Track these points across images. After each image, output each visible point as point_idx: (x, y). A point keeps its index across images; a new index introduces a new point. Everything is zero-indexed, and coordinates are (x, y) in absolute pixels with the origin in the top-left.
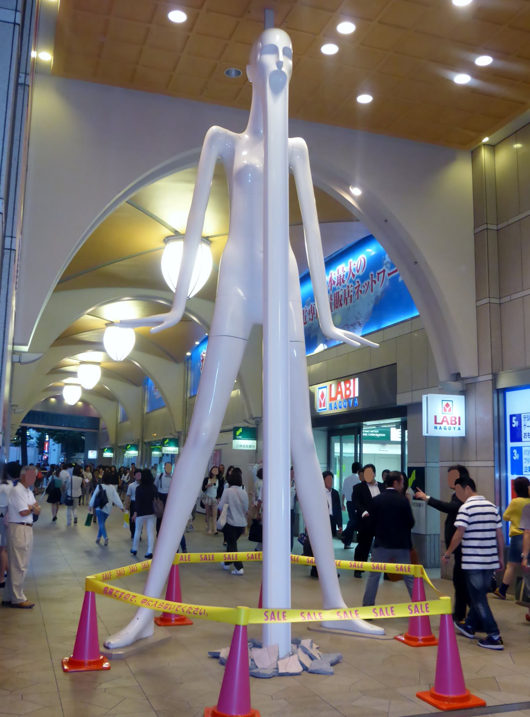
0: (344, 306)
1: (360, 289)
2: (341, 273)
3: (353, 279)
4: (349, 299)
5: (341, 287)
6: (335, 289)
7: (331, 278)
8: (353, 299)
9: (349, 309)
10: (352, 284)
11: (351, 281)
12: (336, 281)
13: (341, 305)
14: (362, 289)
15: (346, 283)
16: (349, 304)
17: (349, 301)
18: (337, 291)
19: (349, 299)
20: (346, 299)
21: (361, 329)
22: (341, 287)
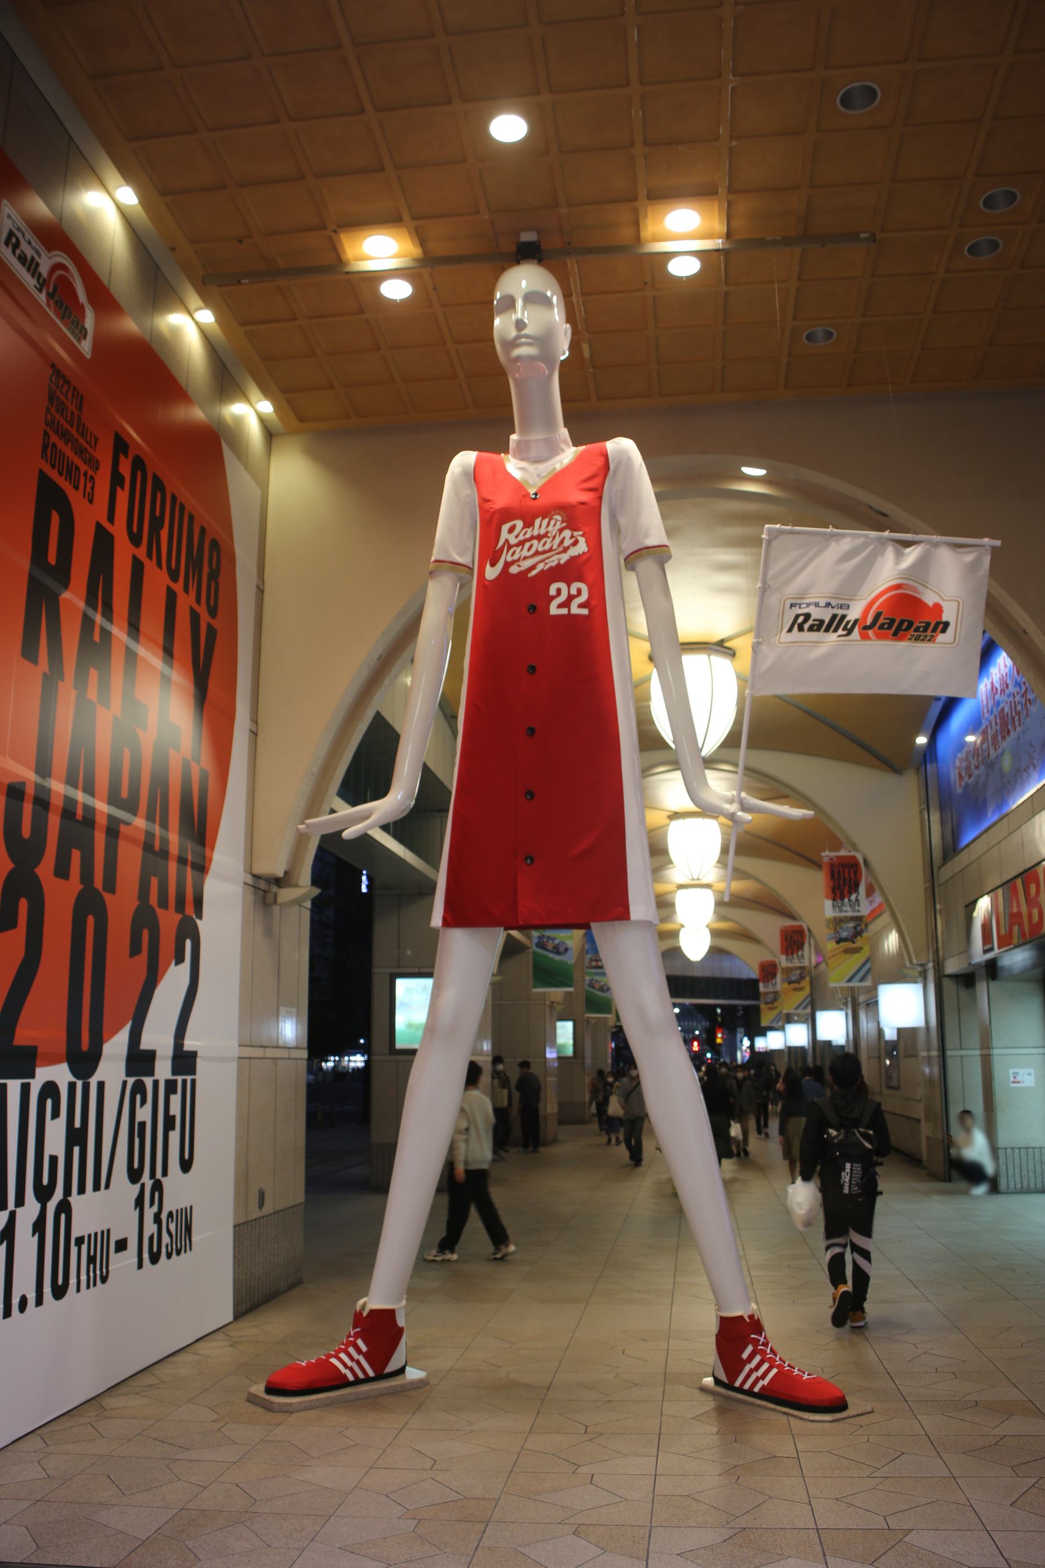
0: (1013, 734)
1: (1029, 696)
2: (1004, 671)
3: (1019, 679)
4: (1017, 718)
5: (1005, 698)
6: (998, 703)
7: (992, 683)
8: (1023, 714)
9: (1018, 739)
10: (1018, 689)
11: (1017, 684)
12: (997, 685)
13: (1009, 732)
14: (1030, 696)
15: (1012, 689)
16: (1018, 729)
17: (1017, 724)
18: (1001, 706)
19: (1017, 718)
20: (1013, 718)
21: (1035, 775)
22: (1005, 698)
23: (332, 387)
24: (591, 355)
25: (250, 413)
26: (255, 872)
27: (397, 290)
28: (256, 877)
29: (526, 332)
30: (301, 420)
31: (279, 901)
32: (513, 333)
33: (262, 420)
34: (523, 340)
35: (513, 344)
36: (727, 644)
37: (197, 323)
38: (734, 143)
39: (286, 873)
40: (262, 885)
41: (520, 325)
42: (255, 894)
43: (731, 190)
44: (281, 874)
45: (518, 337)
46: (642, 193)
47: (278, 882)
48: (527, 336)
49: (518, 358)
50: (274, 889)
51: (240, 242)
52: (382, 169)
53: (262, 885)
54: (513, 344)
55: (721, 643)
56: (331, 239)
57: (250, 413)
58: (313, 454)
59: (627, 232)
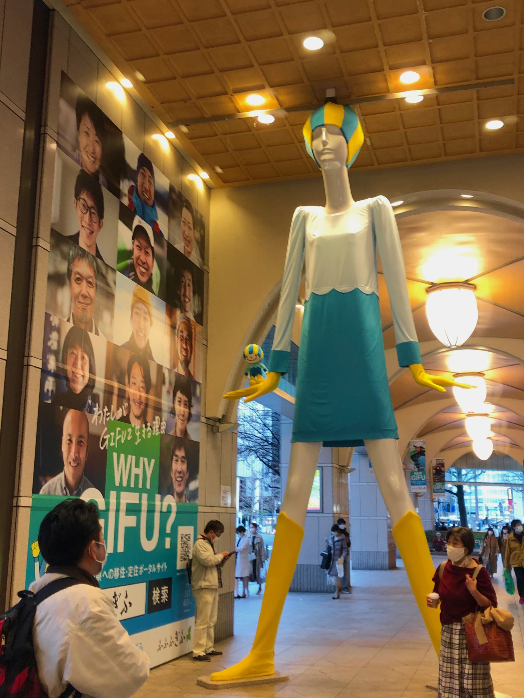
23: (239, 166)
24: (372, 144)
25: (197, 180)
26: (207, 416)
27: (266, 118)
28: (208, 418)
29: (327, 147)
30: (225, 182)
31: (219, 431)
32: (321, 148)
33: (205, 182)
34: (326, 151)
35: (321, 153)
36: (470, 282)
37: (167, 139)
38: (431, 41)
39: (223, 416)
40: (211, 422)
41: (325, 143)
42: (207, 428)
43: (433, 62)
44: (220, 417)
45: (324, 150)
46: (386, 67)
47: (220, 421)
48: (328, 149)
49: (324, 161)
50: (218, 424)
51: (186, 102)
52: (252, 66)
53: (211, 422)
54: (321, 153)
55: (467, 281)
56: (230, 98)
57: (197, 180)
58: (231, 198)
59: (381, 85)
